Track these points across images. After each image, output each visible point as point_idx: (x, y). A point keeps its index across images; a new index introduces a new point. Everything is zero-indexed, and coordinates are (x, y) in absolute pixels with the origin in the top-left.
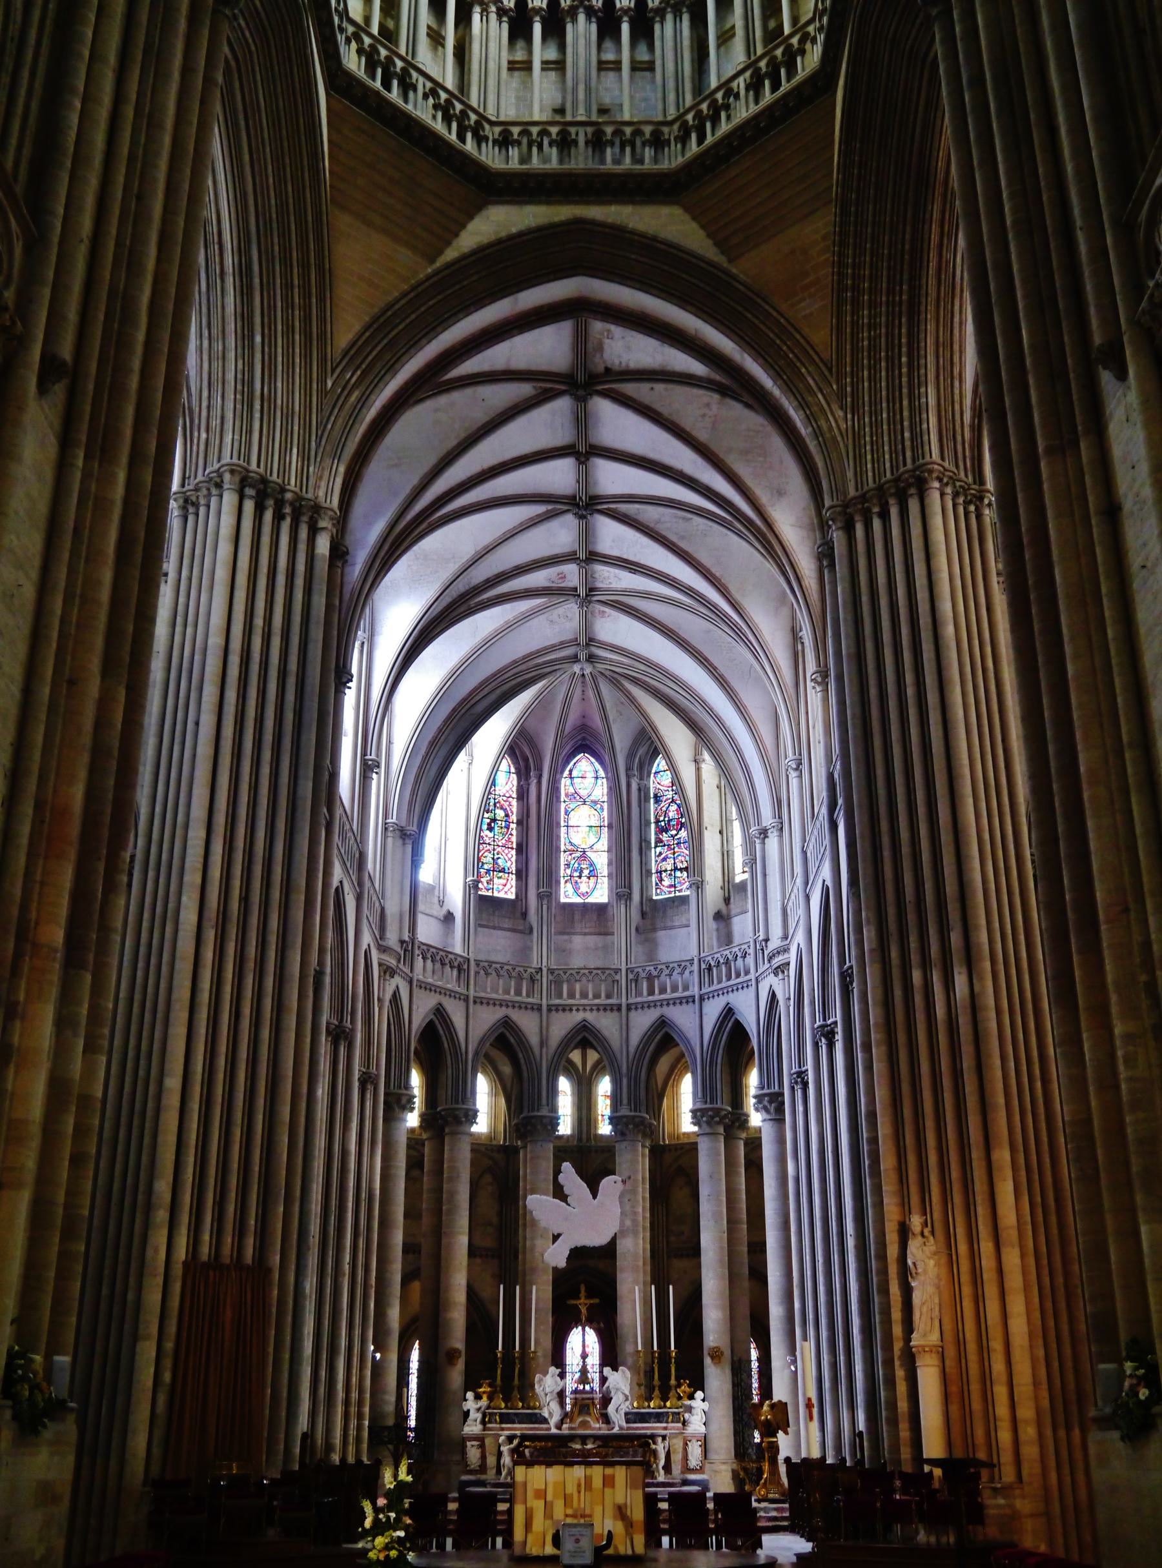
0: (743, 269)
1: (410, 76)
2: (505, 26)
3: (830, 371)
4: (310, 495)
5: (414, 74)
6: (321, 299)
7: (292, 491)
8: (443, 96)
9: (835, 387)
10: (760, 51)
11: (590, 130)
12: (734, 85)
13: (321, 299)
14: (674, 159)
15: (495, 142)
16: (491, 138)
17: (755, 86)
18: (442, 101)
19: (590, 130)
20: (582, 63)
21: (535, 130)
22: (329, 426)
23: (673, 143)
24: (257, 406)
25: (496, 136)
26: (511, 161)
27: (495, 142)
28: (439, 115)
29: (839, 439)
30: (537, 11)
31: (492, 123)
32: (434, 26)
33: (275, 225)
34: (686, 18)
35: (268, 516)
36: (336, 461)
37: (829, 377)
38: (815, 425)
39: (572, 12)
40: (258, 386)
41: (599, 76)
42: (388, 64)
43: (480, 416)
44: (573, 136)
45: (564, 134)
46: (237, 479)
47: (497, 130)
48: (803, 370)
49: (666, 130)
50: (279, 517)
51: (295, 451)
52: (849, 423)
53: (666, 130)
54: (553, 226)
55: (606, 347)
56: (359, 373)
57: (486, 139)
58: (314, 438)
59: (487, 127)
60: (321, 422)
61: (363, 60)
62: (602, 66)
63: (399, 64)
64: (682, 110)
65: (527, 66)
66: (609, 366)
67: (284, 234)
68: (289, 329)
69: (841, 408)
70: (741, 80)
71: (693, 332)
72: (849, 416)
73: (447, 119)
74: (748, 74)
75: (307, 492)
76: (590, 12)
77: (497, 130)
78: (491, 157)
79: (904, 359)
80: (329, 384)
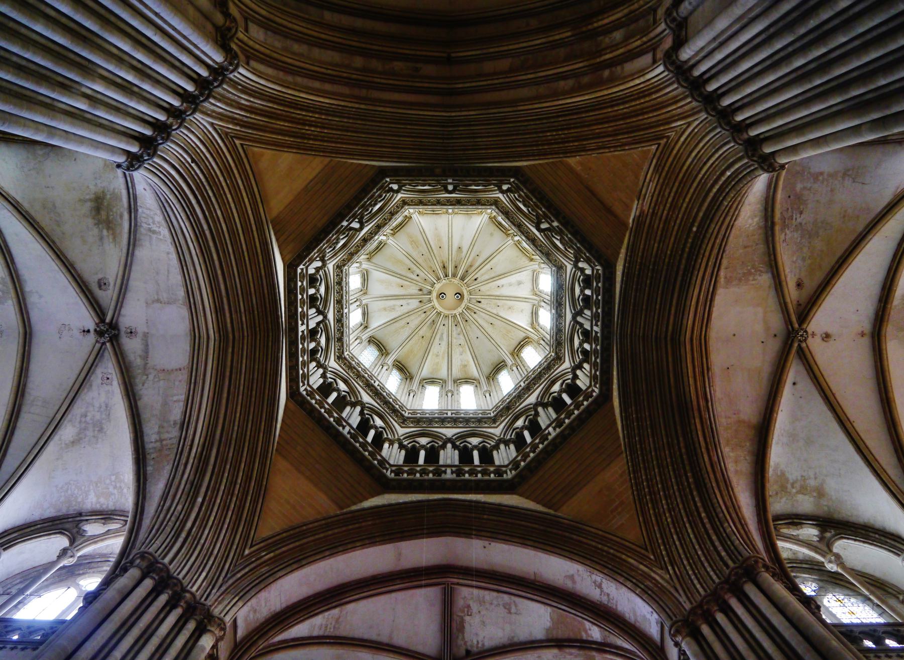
0: (568, 511)
2: (403, 452)
3: (646, 550)
4: (209, 603)
6: (255, 502)
7: (192, 593)
9: (652, 557)
13: (255, 502)
14: (509, 475)
19: (454, 469)
22: (239, 575)
23: (509, 472)
24: (183, 535)
29: (665, 584)
30: (423, 447)
31: (391, 466)
33: (233, 442)
34: (512, 447)
35: (163, 598)
36: (237, 598)
37: (646, 553)
38: (642, 586)
39: (443, 447)
40: (189, 524)
46: (144, 564)
47: (394, 468)
48: (624, 557)
50: (171, 605)
51: (204, 574)
52: (671, 572)
53: (504, 469)
54: (428, 501)
55: (467, 626)
56: (272, 555)
58: (223, 574)
59: (388, 466)
60: (232, 571)
64: (511, 459)
66: (469, 648)
67: (238, 452)
68: (225, 507)
69: (662, 569)
71: (532, 577)
72: (670, 568)
74: (554, 425)
75: (206, 600)
76: (455, 447)
77: (394, 468)
78: (389, 474)
79: (703, 515)
80: (247, 552)
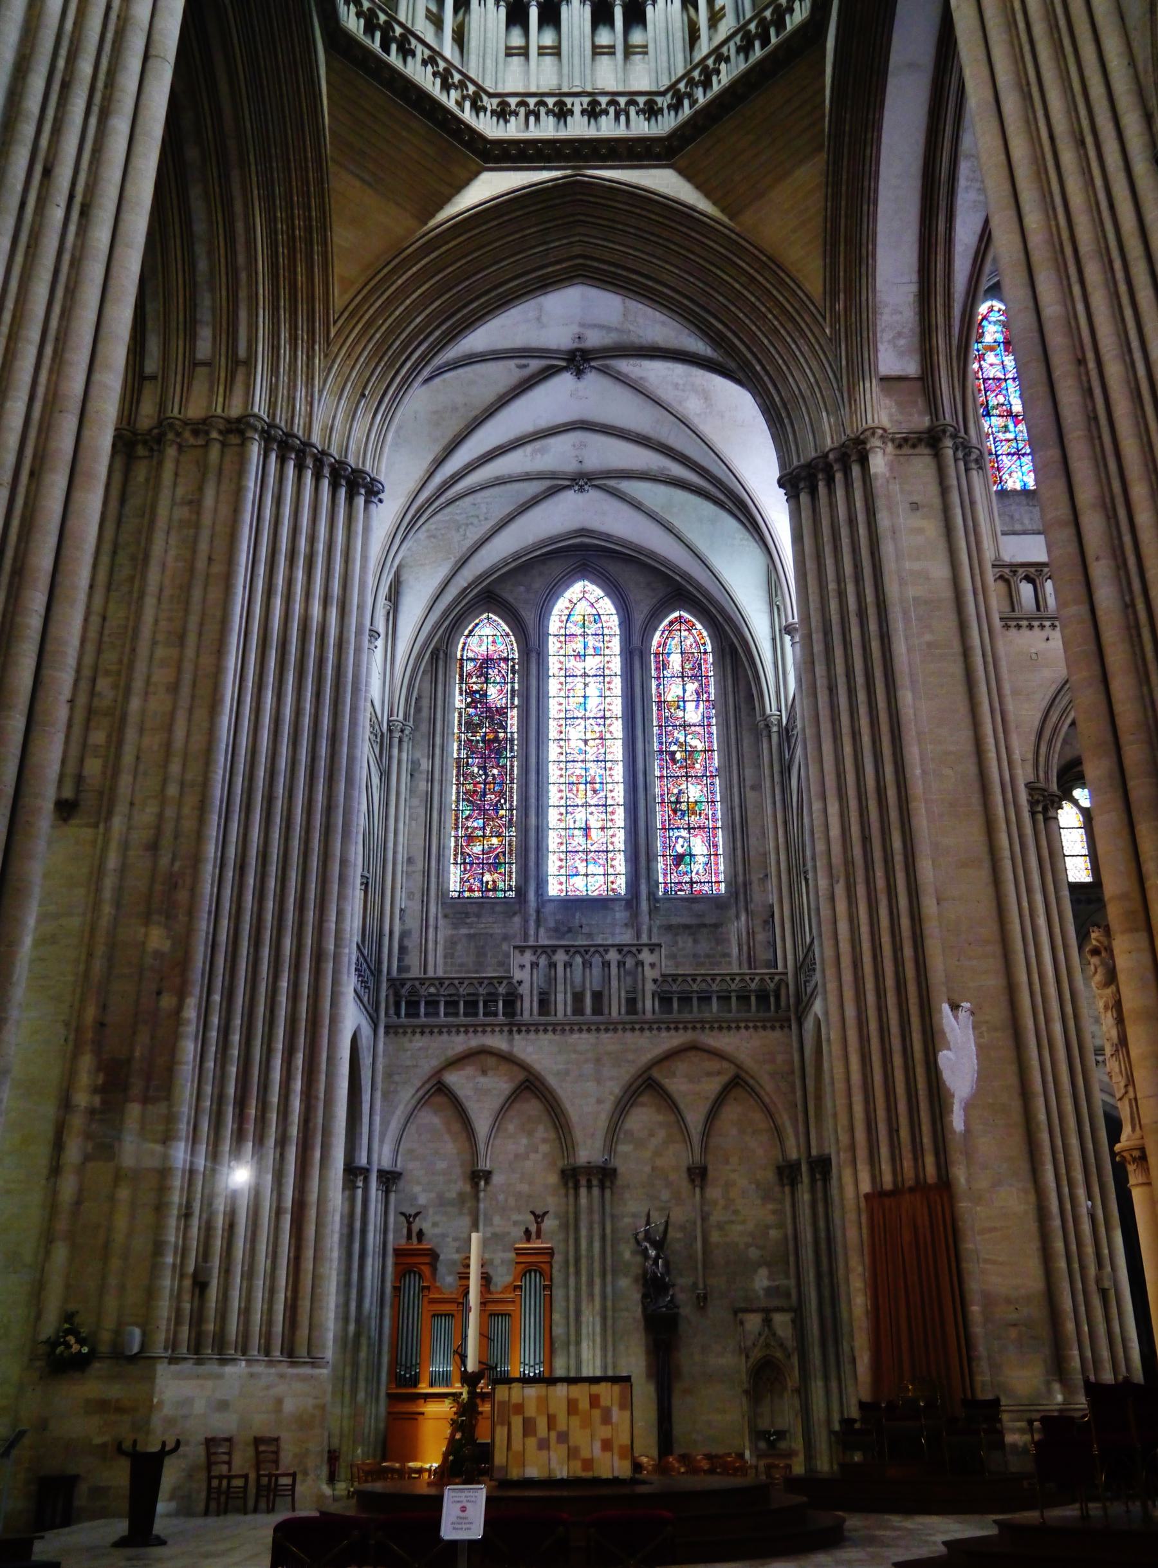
1: (409, 43)
5: (413, 42)
8: (442, 65)
10: (748, 15)
11: (586, 100)
12: (724, 50)
14: (666, 124)
15: (493, 112)
16: (489, 108)
17: (745, 49)
18: (441, 69)
19: (586, 100)
20: (576, 33)
21: (532, 101)
23: (666, 111)
25: (494, 107)
26: (513, 130)
27: (493, 112)
28: (438, 81)
31: (491, 95)
32: (434, 9)
41: (593, 59)
42: (387, 29)
43: (488, 395)
44: (569, 106)
45: (560, 104)
47: (495, 101)
49: (659, 100)
53: (659, 100)
57: (485, 109)
59: (485, 98)
61: (362, 21)
62: (597, 51)
63: (398, 31)
65: (524, 52)
70: (732, 44)
73: (446, 87)
74: (738, 39)
77: (495, 101)
78: (488, 127)
